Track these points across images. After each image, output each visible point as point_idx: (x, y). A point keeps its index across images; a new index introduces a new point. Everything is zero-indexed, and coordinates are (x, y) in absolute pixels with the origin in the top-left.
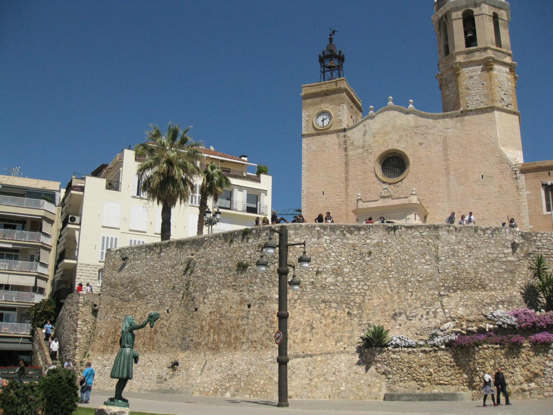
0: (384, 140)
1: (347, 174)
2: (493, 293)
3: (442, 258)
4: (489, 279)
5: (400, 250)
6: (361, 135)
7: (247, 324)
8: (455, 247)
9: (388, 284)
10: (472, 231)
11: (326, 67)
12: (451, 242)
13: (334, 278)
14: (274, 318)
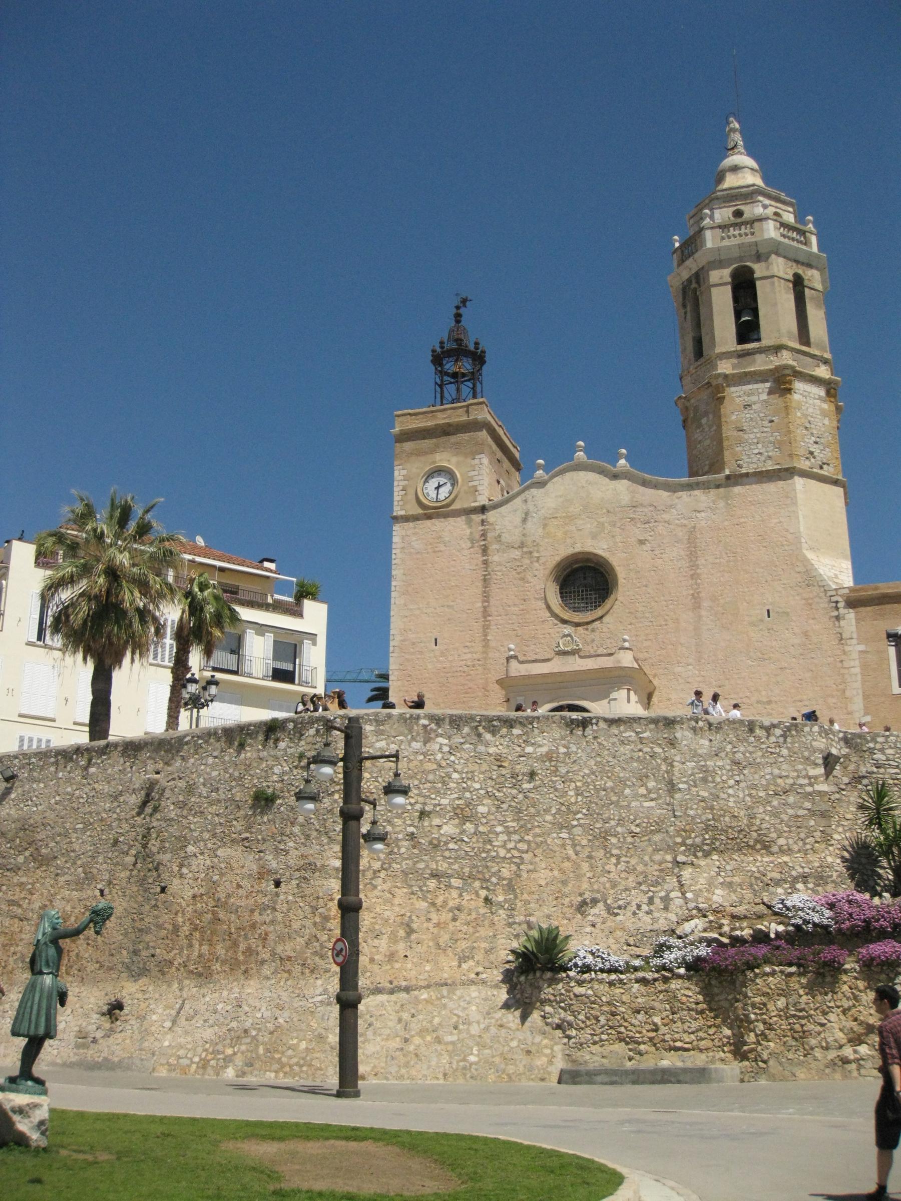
0: (565, 533)
2: (786, 858)
3: (681, 786)
4: (776, 830)
5: (595, 767)
6: (518, 520)
7: (272, 922)
8: (708, 763)
9: (570, 839)
10: (743, 731)
11: (447, 374)
12: (700, 751)
13: (456, 826)
14: (329, 910)
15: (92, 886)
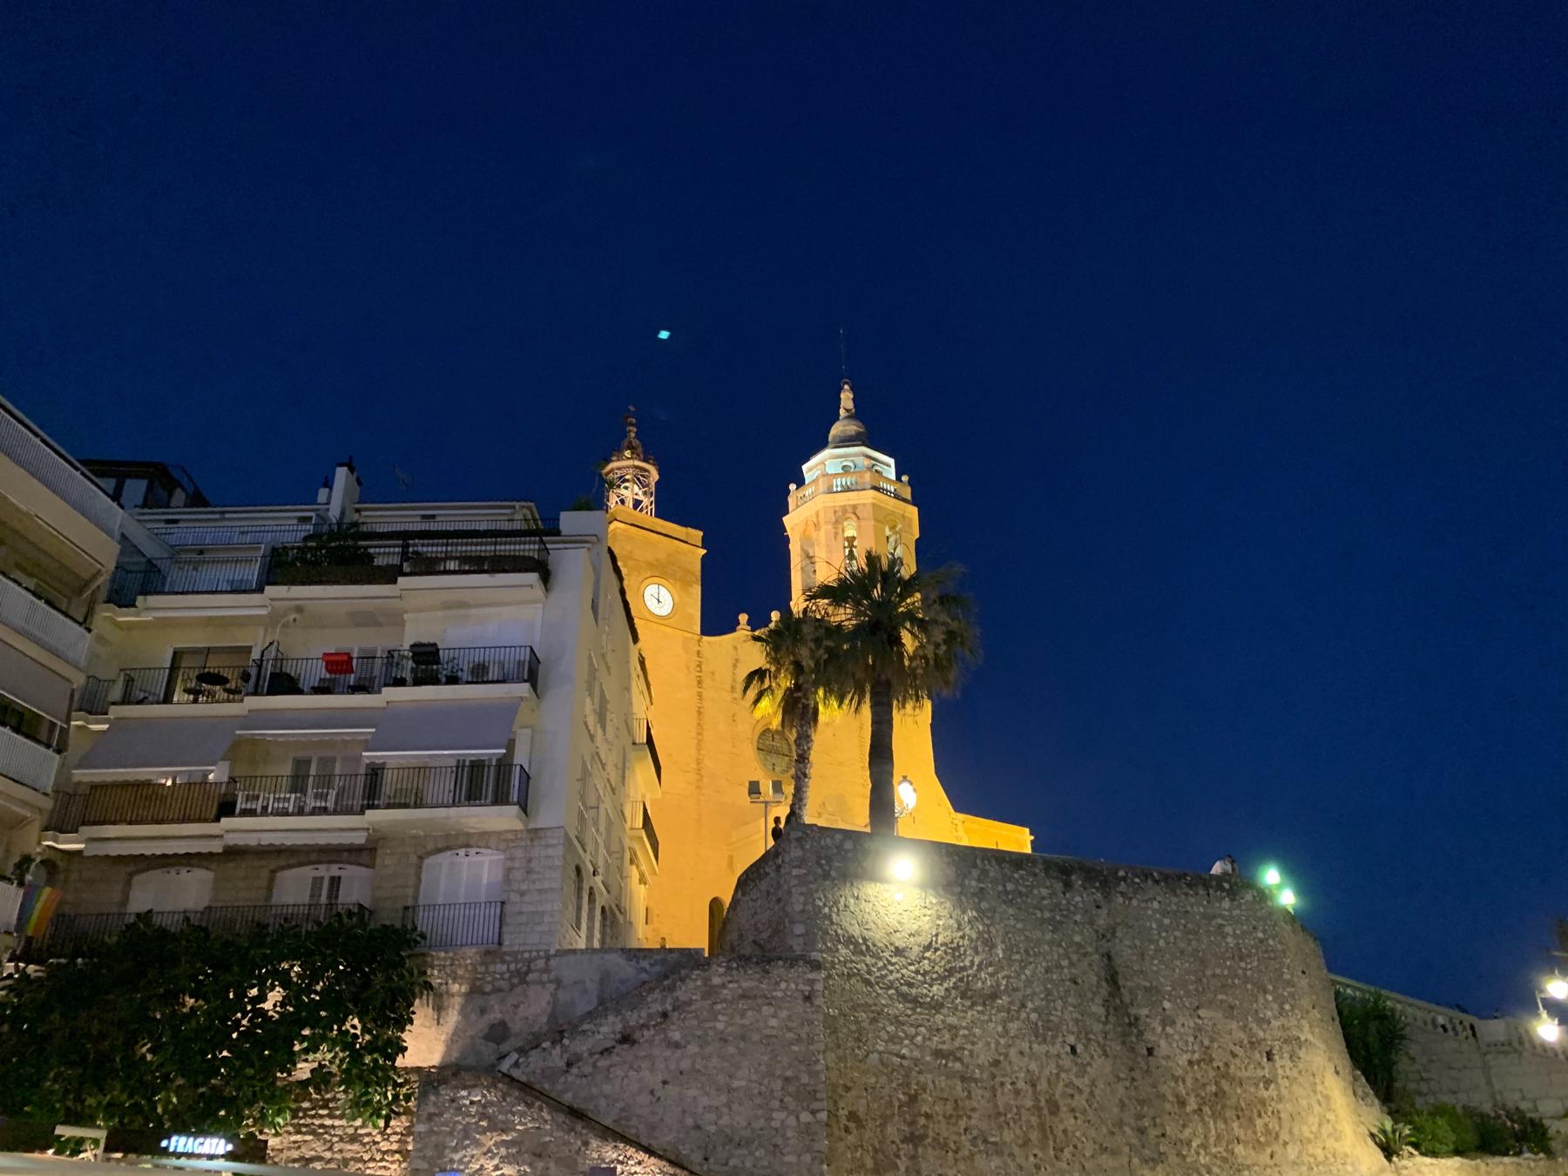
1: (699, 734)
15: (1060, 1039)
